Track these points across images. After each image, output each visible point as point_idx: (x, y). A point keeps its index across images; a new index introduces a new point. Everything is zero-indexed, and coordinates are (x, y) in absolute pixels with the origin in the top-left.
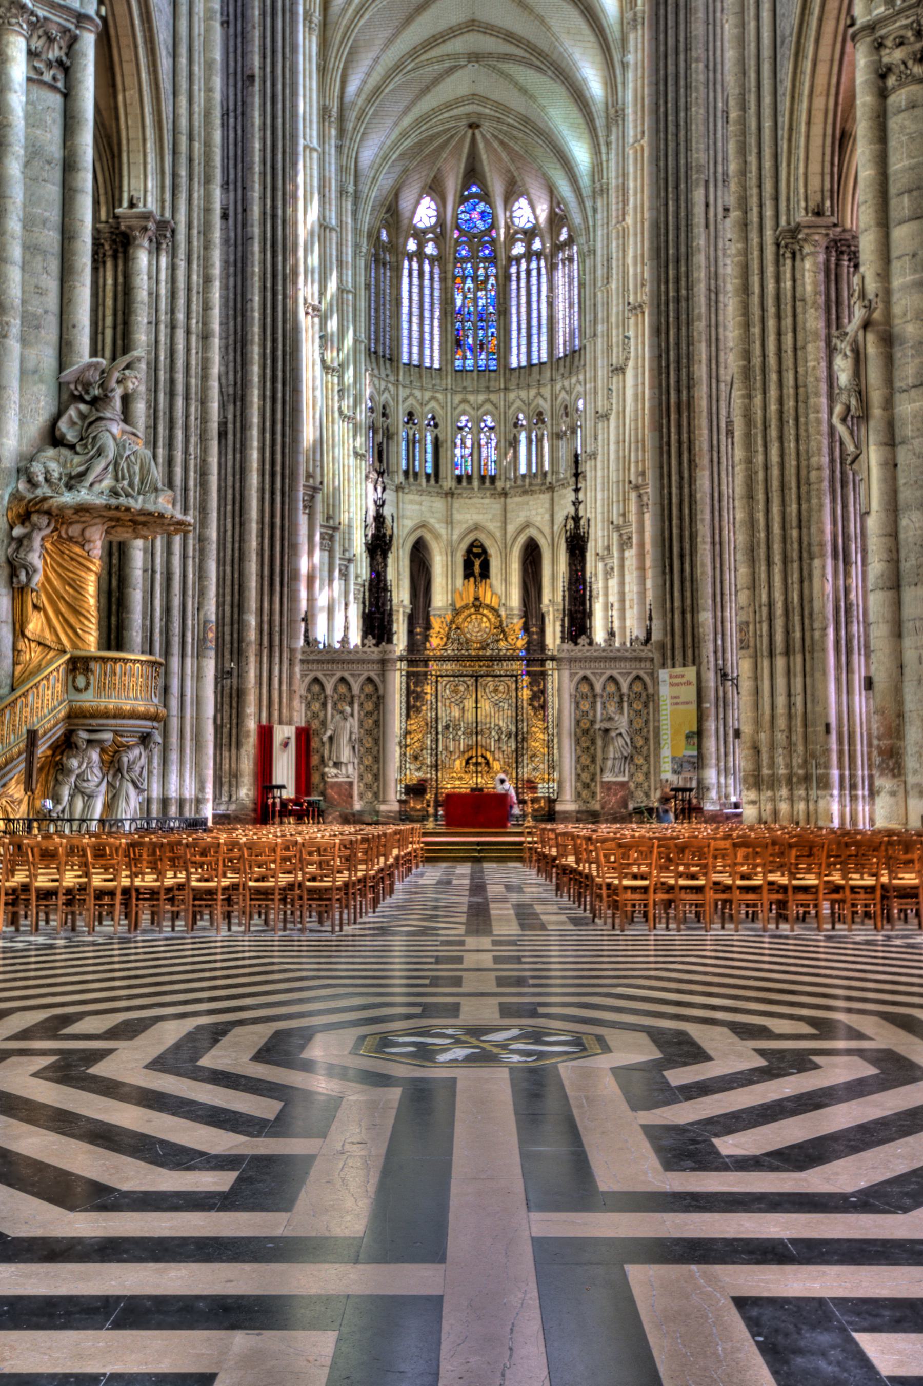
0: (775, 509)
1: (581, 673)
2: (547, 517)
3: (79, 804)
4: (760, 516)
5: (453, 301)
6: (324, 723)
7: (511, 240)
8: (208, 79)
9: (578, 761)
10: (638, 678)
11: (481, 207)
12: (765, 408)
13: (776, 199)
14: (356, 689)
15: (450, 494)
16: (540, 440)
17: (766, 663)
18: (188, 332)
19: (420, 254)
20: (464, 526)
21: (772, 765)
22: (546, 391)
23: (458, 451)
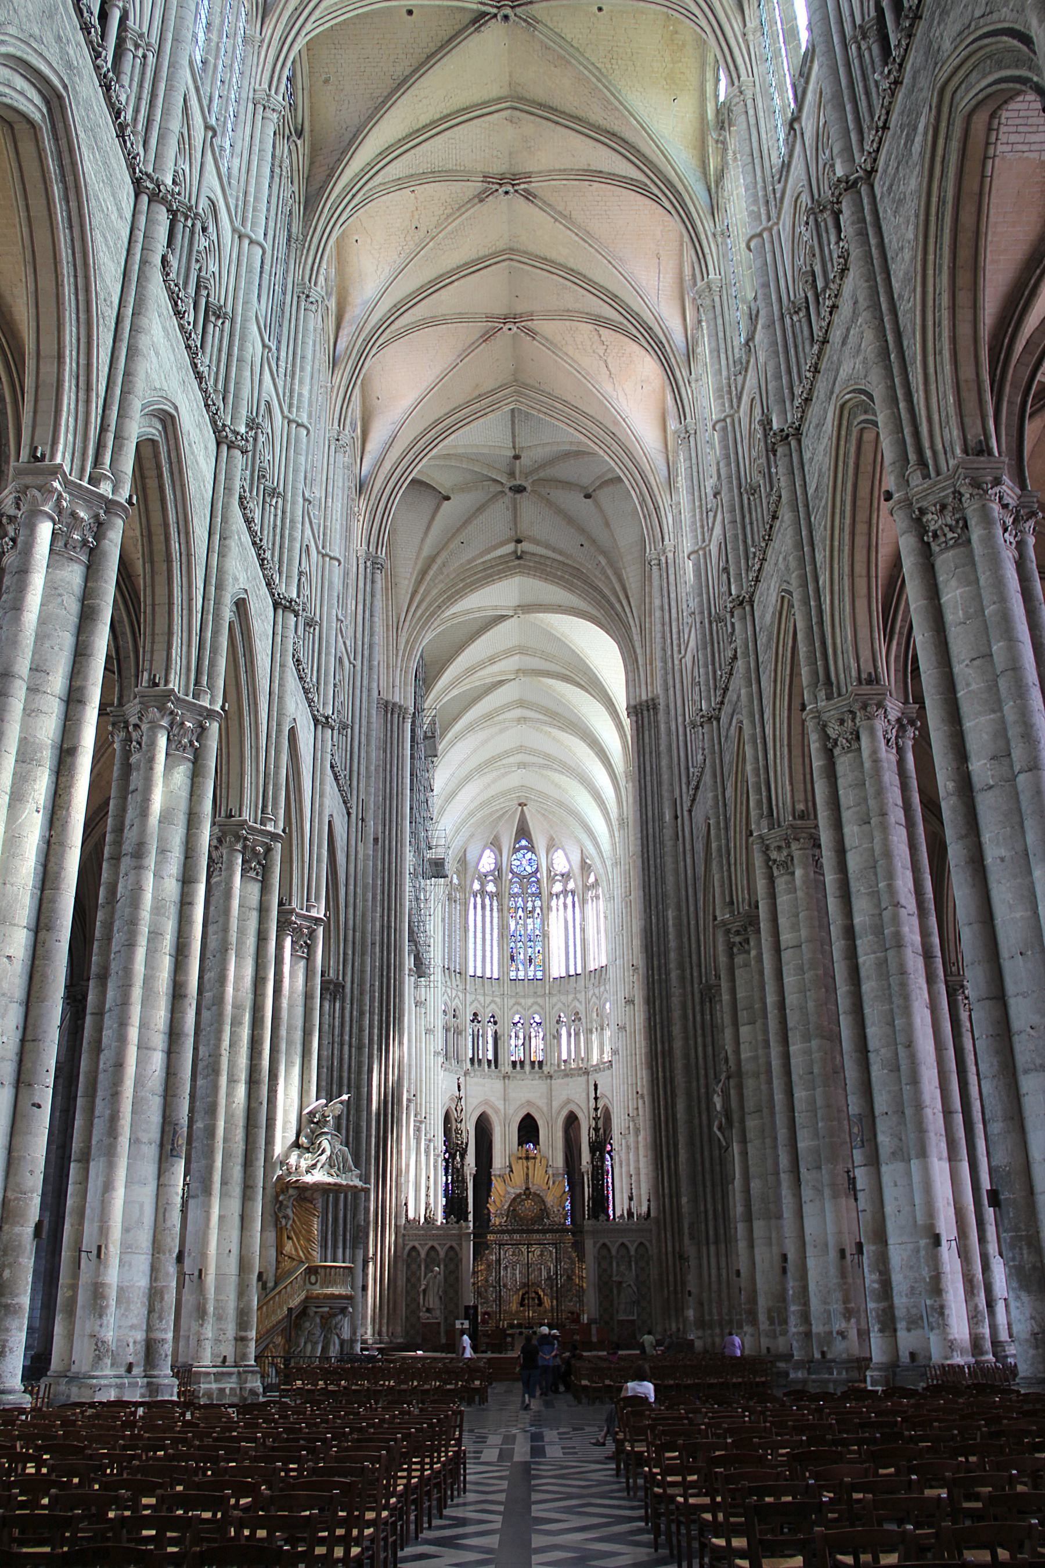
0: (706, 1153)
1: (601, 1241)
2: (584, 1095)
3: (309, 1347)
4: (698, 1156)
5: (508, 925)
6: (419, 1279)
7: (551, 879)
8: (364, 895)
9: (600, 1304)
10: (641, 1244)
11: (529, 855)
12: (698, 1090)
13: (700, 966)
14: (442, 1254)
15: (506, 1077)
16: (577, 1034)
17: (704, 1249)
18: (350, 1046)
19: (483, 892)
20: (519, 1103)
21: (711, 1313)
22: (581, 996)
23: (513, 1042)
